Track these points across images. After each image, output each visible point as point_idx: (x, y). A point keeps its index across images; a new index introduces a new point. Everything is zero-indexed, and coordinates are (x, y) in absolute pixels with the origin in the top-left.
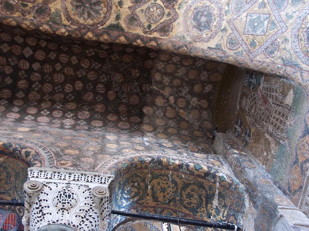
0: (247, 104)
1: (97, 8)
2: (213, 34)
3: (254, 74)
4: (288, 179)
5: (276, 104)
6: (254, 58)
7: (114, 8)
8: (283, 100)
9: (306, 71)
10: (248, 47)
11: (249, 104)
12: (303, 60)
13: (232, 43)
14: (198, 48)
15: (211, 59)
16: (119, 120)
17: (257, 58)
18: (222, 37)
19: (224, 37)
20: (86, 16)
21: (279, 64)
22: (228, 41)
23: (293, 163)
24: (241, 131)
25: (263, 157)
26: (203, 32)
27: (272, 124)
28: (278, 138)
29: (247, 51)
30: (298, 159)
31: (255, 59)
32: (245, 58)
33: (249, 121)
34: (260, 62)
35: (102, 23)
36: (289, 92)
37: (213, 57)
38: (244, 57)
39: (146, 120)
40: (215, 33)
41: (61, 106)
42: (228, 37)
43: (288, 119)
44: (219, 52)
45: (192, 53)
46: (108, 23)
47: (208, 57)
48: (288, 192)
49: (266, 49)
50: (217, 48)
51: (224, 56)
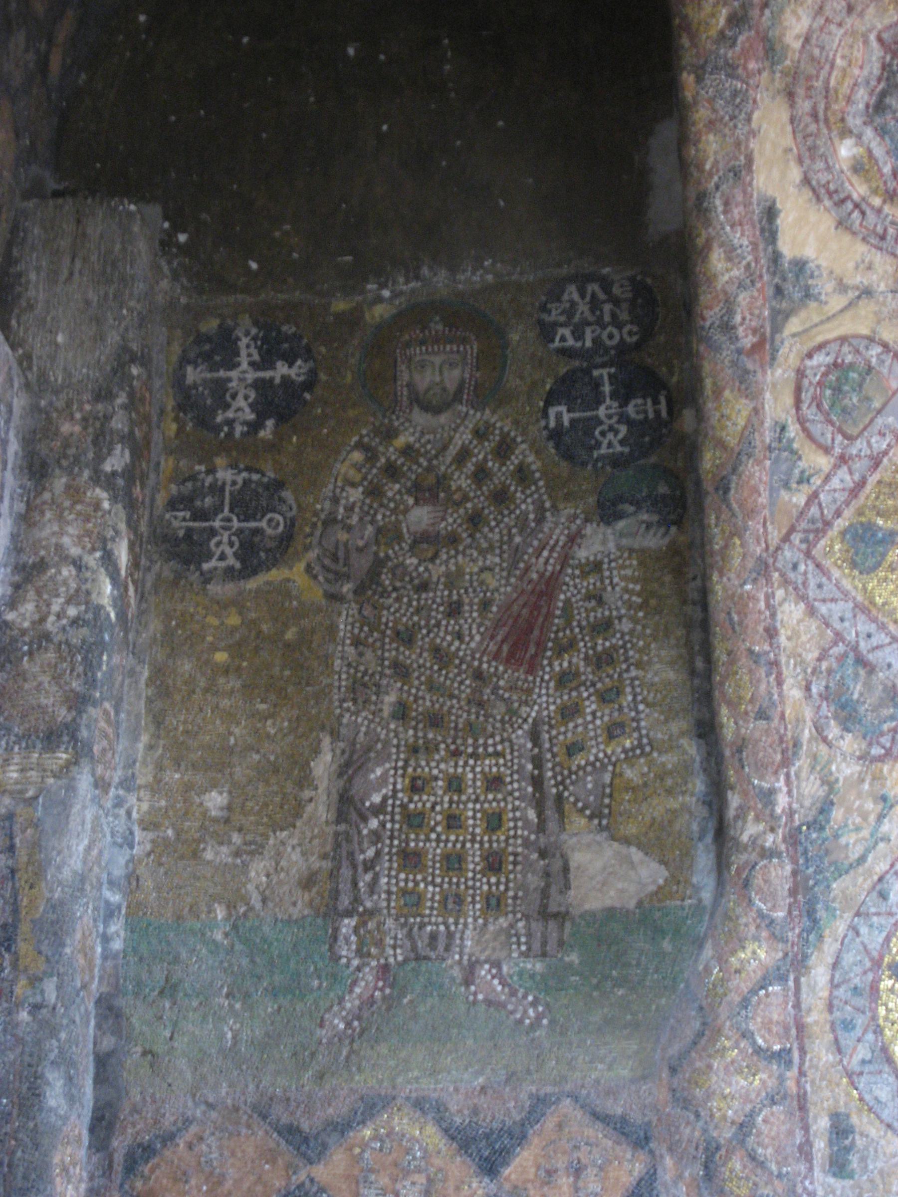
0: (437, 411)
2: (871, 217)
3: (656, 402)
4: (188, 1122)
5: (538, 762)
6: (786, 582)
8: (581, 811)
9: (797, 1005)
10: (838, 514)
11: (445, 448)
12: (848, 958)
14: (749, 120)
15: (700, 242)
17: (785, 606)
18: (867, 292)
19: (866, 308)
21: (789, 793)
22: (846, 349)
23: (285, 1120)
24: (239, 430)
25: (188, 787)
26: (869, 133)
27: (416, 787)
28: (355, 884)
29: (814, 510)
30: (325, 1146)
31: (780, 593)
32: (766, 512)
33: (335, 500)
34: (771, 633)
36: (639, 846)
37: (717, 260)
38: (772, 503)
40: (879, 229)
42: (871, 339)
43: (491, 928)
44: (760, 302)
45: (699, 80)
47: (708, 223)
48: (120, 1144)
49: (861, 661)
50: (784, 279)
51: (739, 352)
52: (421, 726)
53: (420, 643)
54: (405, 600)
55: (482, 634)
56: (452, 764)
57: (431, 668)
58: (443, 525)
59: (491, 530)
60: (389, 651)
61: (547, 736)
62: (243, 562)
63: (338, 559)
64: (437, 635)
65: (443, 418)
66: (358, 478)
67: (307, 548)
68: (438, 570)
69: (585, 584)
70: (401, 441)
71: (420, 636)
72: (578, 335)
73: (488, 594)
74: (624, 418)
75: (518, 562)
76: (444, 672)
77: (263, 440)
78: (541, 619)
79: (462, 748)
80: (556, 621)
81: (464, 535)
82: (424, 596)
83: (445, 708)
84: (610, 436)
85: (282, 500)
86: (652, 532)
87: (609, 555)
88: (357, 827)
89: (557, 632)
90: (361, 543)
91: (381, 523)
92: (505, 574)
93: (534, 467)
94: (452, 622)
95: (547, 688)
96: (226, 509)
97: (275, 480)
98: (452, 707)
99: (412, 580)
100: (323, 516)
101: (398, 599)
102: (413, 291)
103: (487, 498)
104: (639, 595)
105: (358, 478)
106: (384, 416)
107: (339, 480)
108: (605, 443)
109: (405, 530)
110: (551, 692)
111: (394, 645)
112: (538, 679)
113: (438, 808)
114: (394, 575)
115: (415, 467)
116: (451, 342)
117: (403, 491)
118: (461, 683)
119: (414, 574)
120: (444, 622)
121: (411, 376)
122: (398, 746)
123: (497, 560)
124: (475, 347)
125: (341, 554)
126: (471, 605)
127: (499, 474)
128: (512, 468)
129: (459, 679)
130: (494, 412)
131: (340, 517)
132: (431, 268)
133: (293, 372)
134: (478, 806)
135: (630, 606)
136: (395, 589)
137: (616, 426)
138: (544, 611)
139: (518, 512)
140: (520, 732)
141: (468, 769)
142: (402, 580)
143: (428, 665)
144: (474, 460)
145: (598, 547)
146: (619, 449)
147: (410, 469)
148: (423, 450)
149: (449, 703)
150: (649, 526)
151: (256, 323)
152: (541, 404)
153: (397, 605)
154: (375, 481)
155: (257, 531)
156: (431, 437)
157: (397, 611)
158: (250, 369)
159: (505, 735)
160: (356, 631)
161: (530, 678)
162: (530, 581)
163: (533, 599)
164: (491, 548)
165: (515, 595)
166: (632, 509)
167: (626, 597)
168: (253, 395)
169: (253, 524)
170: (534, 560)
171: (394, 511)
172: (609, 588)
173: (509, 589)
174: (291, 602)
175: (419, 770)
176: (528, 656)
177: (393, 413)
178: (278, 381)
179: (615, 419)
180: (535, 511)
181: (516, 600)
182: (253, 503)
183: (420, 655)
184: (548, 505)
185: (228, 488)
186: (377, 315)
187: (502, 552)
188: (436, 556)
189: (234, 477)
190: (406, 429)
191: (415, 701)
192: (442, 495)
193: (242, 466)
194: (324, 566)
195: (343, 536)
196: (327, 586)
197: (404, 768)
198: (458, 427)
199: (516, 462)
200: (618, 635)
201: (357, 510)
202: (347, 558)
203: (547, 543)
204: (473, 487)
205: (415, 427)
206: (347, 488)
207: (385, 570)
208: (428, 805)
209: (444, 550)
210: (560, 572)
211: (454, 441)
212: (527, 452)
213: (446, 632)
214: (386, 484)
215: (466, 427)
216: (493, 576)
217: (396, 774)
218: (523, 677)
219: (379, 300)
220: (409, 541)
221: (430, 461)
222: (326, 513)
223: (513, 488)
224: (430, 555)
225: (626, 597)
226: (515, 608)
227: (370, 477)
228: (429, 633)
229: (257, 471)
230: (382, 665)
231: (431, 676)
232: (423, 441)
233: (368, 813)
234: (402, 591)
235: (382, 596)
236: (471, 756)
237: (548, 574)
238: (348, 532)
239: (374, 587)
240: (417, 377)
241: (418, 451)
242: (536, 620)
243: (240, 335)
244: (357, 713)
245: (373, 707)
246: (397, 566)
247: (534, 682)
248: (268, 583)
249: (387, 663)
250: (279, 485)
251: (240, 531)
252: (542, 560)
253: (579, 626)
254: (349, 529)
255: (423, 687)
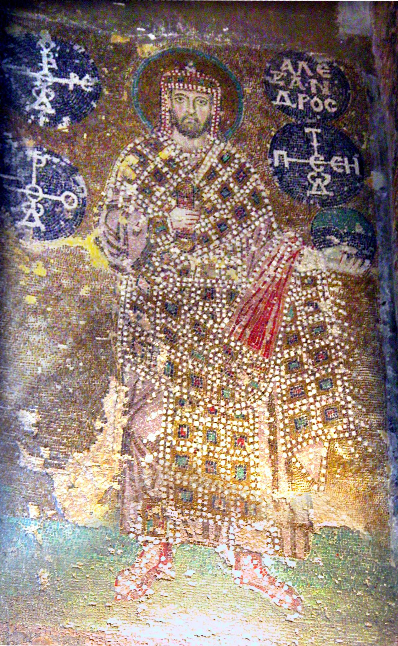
0: (192, 135)
11: (198, 166)
24: (43, 120)
33: (117, 191)
52: (185, 384)
53: (183, 317)
54: (171, 280)
55: (230, 318)
56: (209, 419)
57: (192, 338)
58: (198, 226)
59: (234, 236)
60: (160, 319)
61: (280, 409)
62: (47, 225)
63: (119, 238)
64: (196, 313)
65: (196, 142)
66: (133, 176)
67: (97, 224)
68: (194, 261)
69: (305, 293)
70: (165, 154)
71: (183, 312)
72: (294, 100)
73: (234, 287)
74: (329, 170)
75: (255, 267)
76: (202, 343)
77: (61, 132)
78: (273, 315)
79: (216, 408)
80: (285, 318)
81: (214, 238)
82: (185, 280)
83: (203, 373)
84: (319, 181)
85: (75, 182)
86: (352, 261)
87: (321, 274)
88: (138, 459)
89: (285, 327)
90: (137, 229)
91: (151, 216)
92: (245, 273)
93: (264, 194)
94: (207, 304)
95: (280, 371)
96: (34, 181)
97: (70, 165)
98: (208, 373)
99: (176, 265)
100: (107, 202)
101: (165, 279)
102: (173, 39)
103: (230, 211)
104: (344, 308)
105: (133, 176)
106: (152, 132)
107: (119, 174)
108: (315, 185)
109: (169, 225)
110: (283, 374)
111: (163, 315)
112: (272, 362)
113: (199, 454)
114: (162, 259)
115: (176, 177)
116: (202, 85)
117: (168, 193)
118: (215, 354)
119: (178, 261)
120: (201, 304)
121: (172, 105)
122: (168, 397)
123: (239, 262)
124: (219, 91)
125: (121, 235)
126: (221, 293)
127: (239, 195)
128: (248, 191)
129: (213, 351)
130: (234, 145)
131: (120, 206)
132: (184, 25)
133: (83, 83)
134: (229, 458)
135: (338, 316)
136: (163, 270)
137: (323, 174)
138: (275, 308)
139: (253, 227)
140: (259, 402)
141: (221, 426)
142: (168, 264)
143: (190, 335)
144: (220, 180)
145: (312, 266)
146: (325, 192)
147: (172, 177)
148: (181, 164)
149: (206, 369)
150: (349, 256)
151: (54, 39)
152: (268, 146)
153: (165, 284)
154: (147, 182)
155: (57, 204)
156: (188, 155)
157: (165, 288)
158: (49, 74)
159: (249, 402)
160: (134, 298)
161: (267, 361)
162: (265, 282)
163: (267, 297)
164: (234, 251)
165: (254, 292)
166: (337, 241)
167: (335, 309)
168: (53, 95)
169: (53, 197)
170: (266, 267)
171: (161, 208)
172: (322, 299)
173: (249, 286)
174: (84, 266)
175: (185, 420)
176: (264, 342)
177: (159, 130)
178: (71, 88)
179: (322, 169)
180: (266, 229)
181: (254, 295)
182: (55, 180)
183: (184, 326)
184: (275, 226)
185: (35, 165)
186: (146, 51)
187: (244, 256)
188: (192, 251)
189: (40, 157)
190: (169, 145)
191: (180, 363)
192: (197, 203)
193: (45, 150)
194: (108, 242)
195: (123, 221)
196: (111, 258)
197: (173, 416)
198: (208, 151)
199: (251, 187)
200: (330, 338)
201: (132, 202)
202: (126, 239)
203: (276, 256)
204: (220, 201)
205: (175, 145)
206: (125, 183)
207: (155, 254)
208: (192, 450)
209: (199, 247)
210: (286, 280)
211: (204, 162)
212: (259, 182)
213: (203, 311)
214: (154, 185)
215: (214, 153)
216: (237, 274)
217: (166, 420)
218: (261, 358)
219: (148, 41)
220: (173, 234)
221: (187, 173)
222: (109, 200)
223: (249, 208)
224: (188, 247)
225: (335, 309)
226: (254, 301)
227: (142, 178)
228: (189, 310)
229: (57, 156)
230: (155, 329)
231: (192, 345)
232: (181, 157)
233: (145, 449)
234: (168, 273)
235: (153, 275)
236: (223, 414)
237: (277, 280)
238: (126, 218)
239: (147, 266)
240: (176, 106)
241: (177, 164)
242: (270, 314)
243: (42, 46)
244: (136, 364)
245: (148, 363)
246: (164, 252)
247: (268, 363)
248: (66, 247)
249: (158, 328)
250: (74, 170)
251: (46, 201)
252: (272, 268)
253: (301, 325)
254: (127, 215)
255: (186, 353)
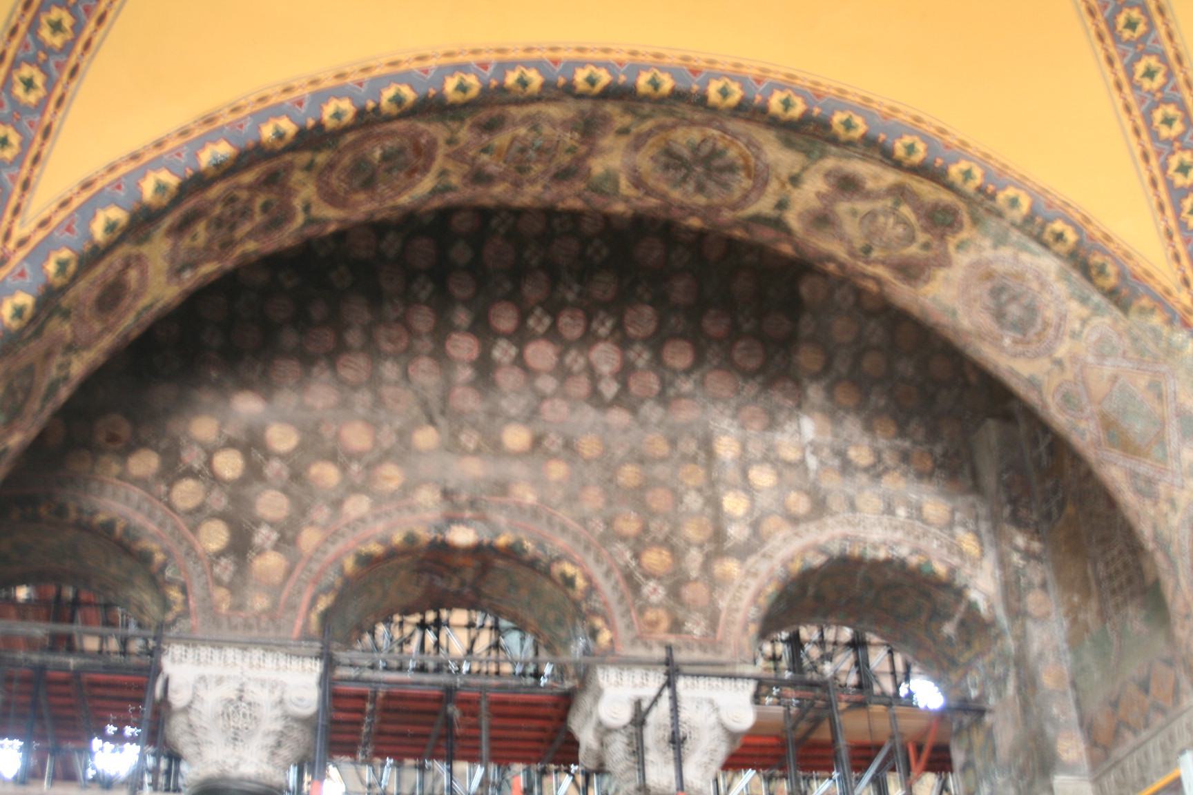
1: (726, 176)
7: (774, 186)
13: (1067, 400)
16: (735, 334)
20: (690, 187)
35: (734, 207)
39: (807, 325)
41: (576, 288)
46: (751, 210)
